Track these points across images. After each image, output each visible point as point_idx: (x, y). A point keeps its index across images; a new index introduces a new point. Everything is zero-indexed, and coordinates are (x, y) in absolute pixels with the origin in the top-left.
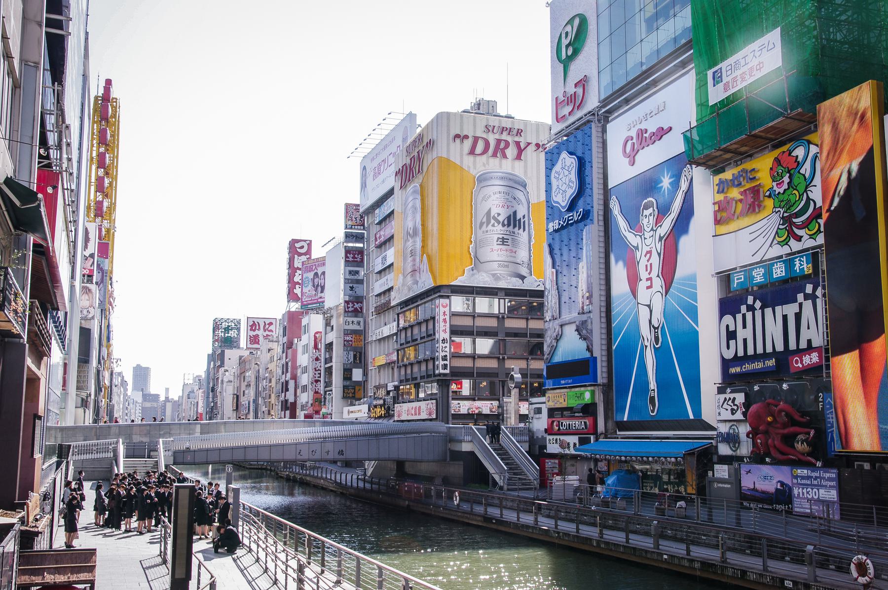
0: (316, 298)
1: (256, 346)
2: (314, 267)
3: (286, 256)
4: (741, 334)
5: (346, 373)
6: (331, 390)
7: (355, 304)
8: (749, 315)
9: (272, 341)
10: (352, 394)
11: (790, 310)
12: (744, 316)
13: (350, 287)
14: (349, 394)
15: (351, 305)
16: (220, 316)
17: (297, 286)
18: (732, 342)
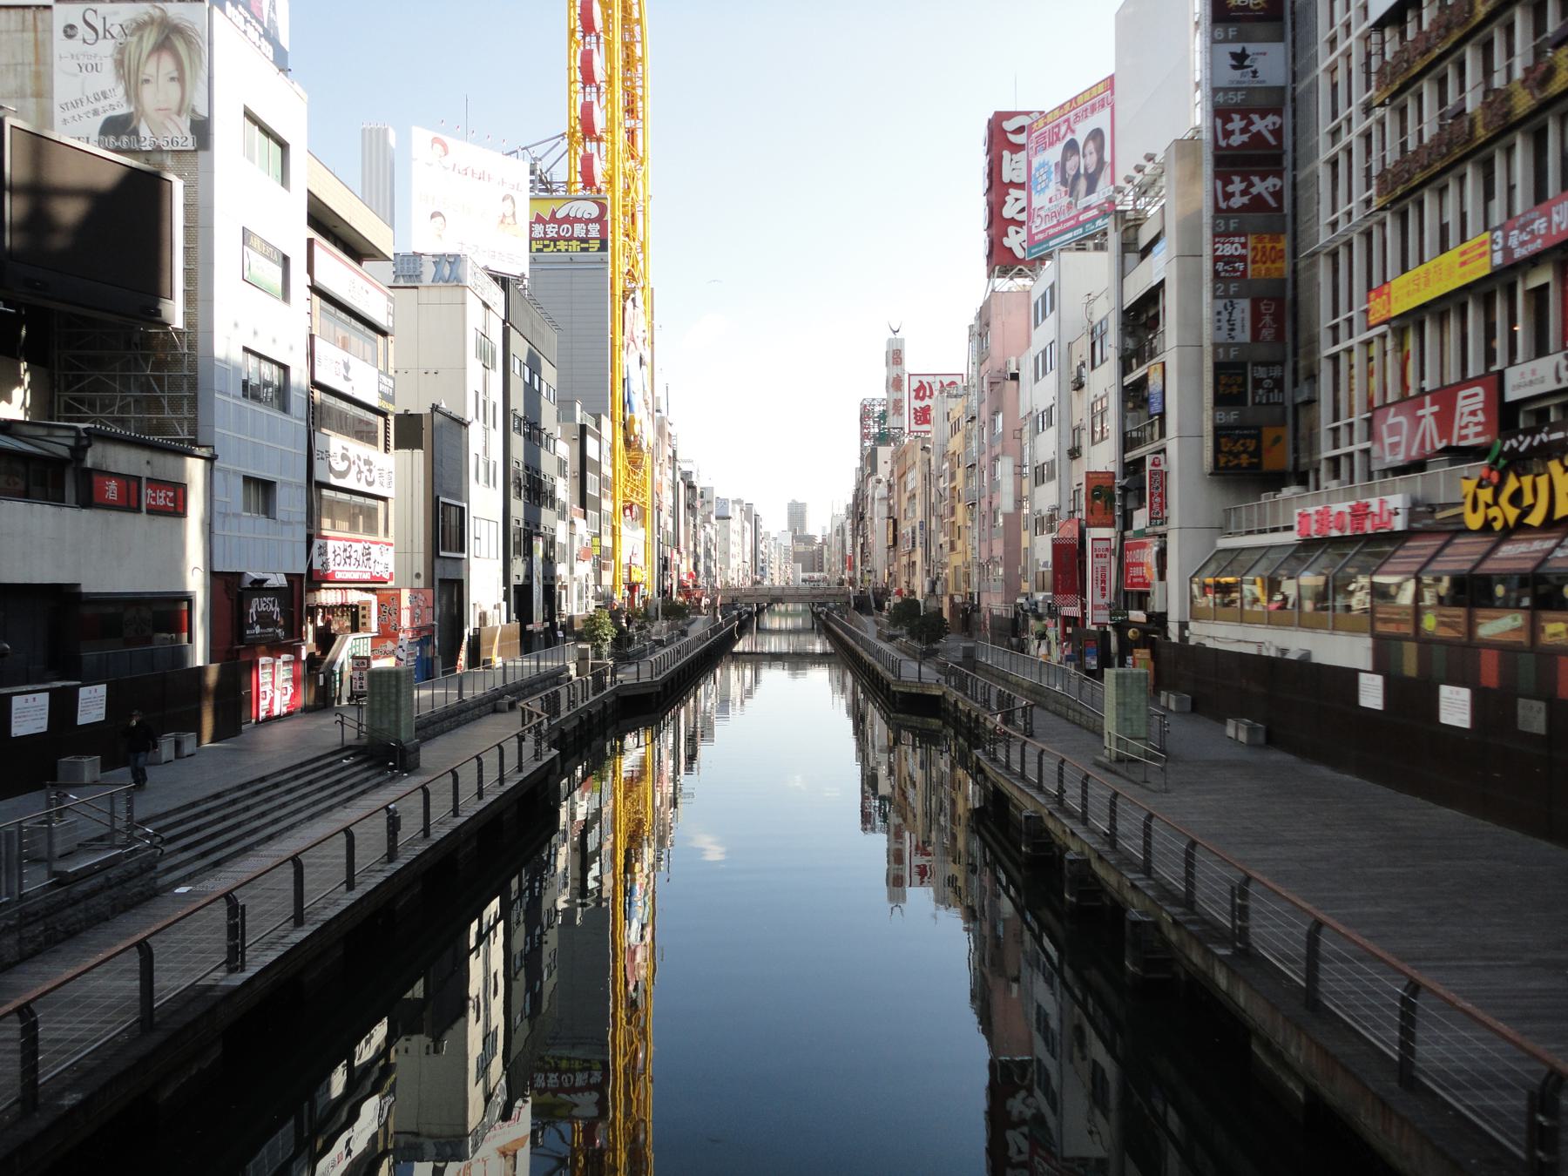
0: (1074, 212)
1: (926, 427)
2: (1063, 129)
3: (981, 162)
5: (1223, 380)
6: (1164, 451)
7: (1255, 117)
9: (956, 396)
10: (1251, 455)
13: (1234, 55)
14: (1237, 455)
15: (1237, 123)
16: (870, 396)
17: (1011, 229)
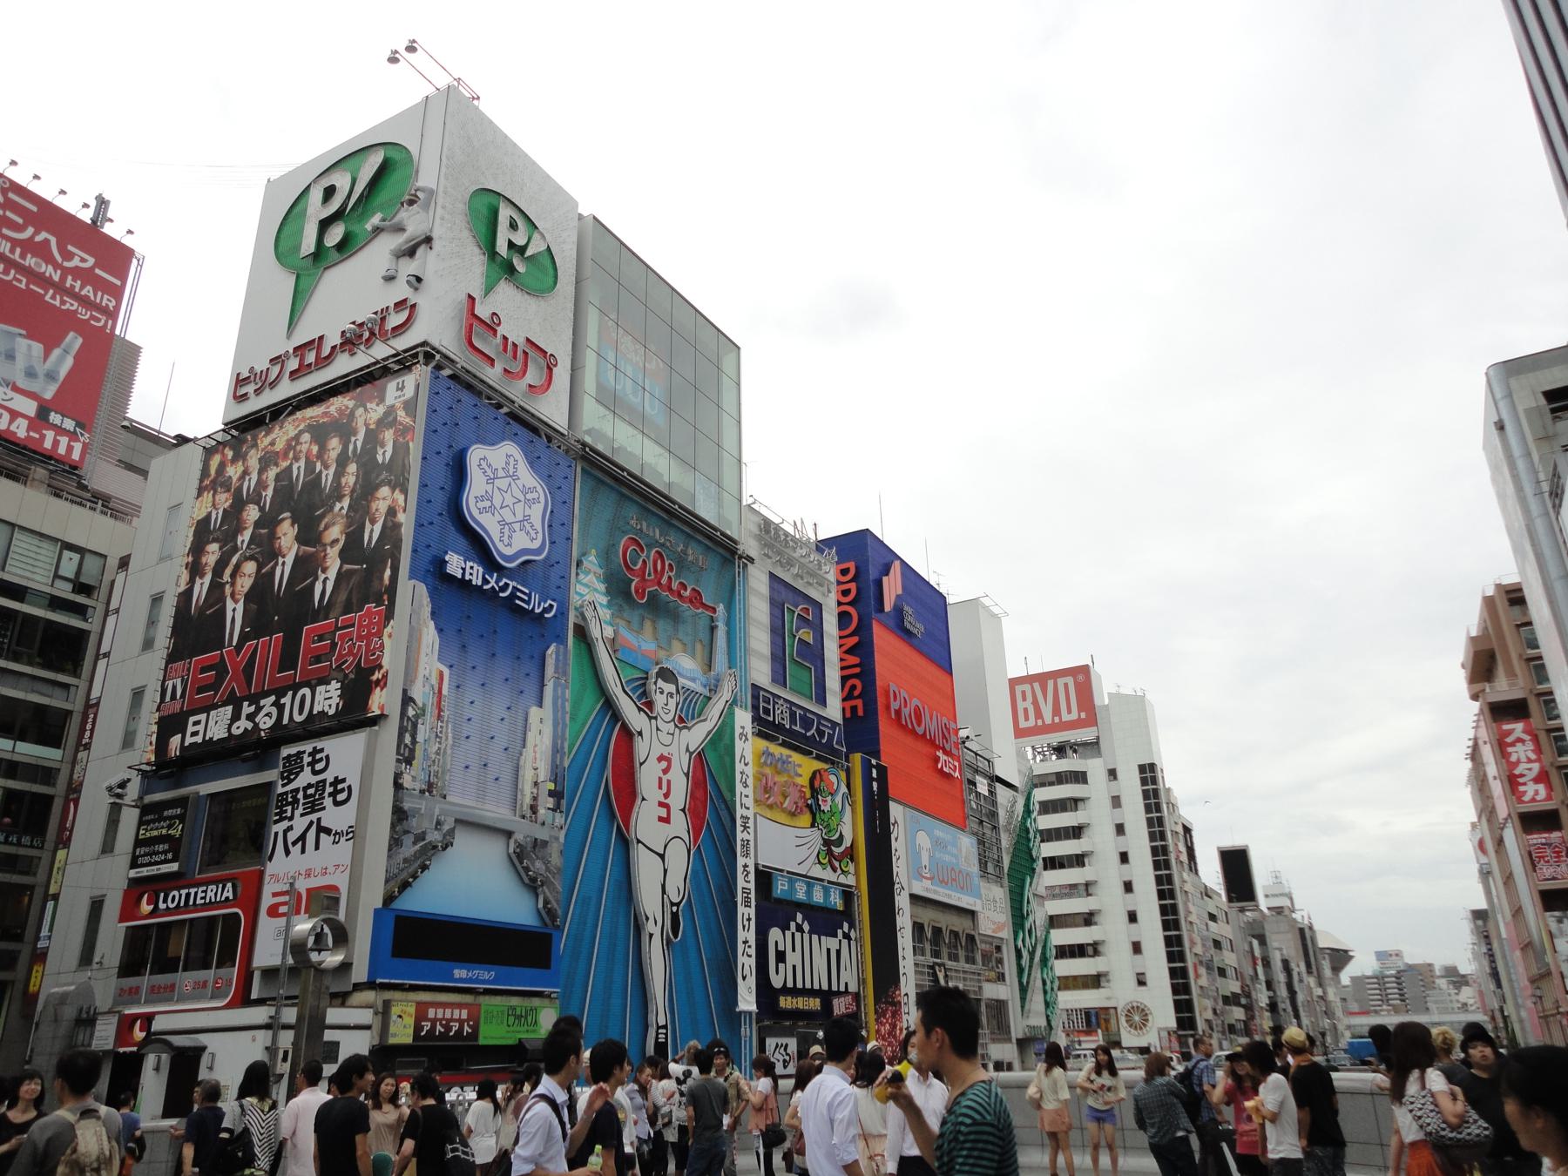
4: (793, 958)
8: (798, 935)
11: (832, 943)
12: (793, 934)
18: (781, 966)
